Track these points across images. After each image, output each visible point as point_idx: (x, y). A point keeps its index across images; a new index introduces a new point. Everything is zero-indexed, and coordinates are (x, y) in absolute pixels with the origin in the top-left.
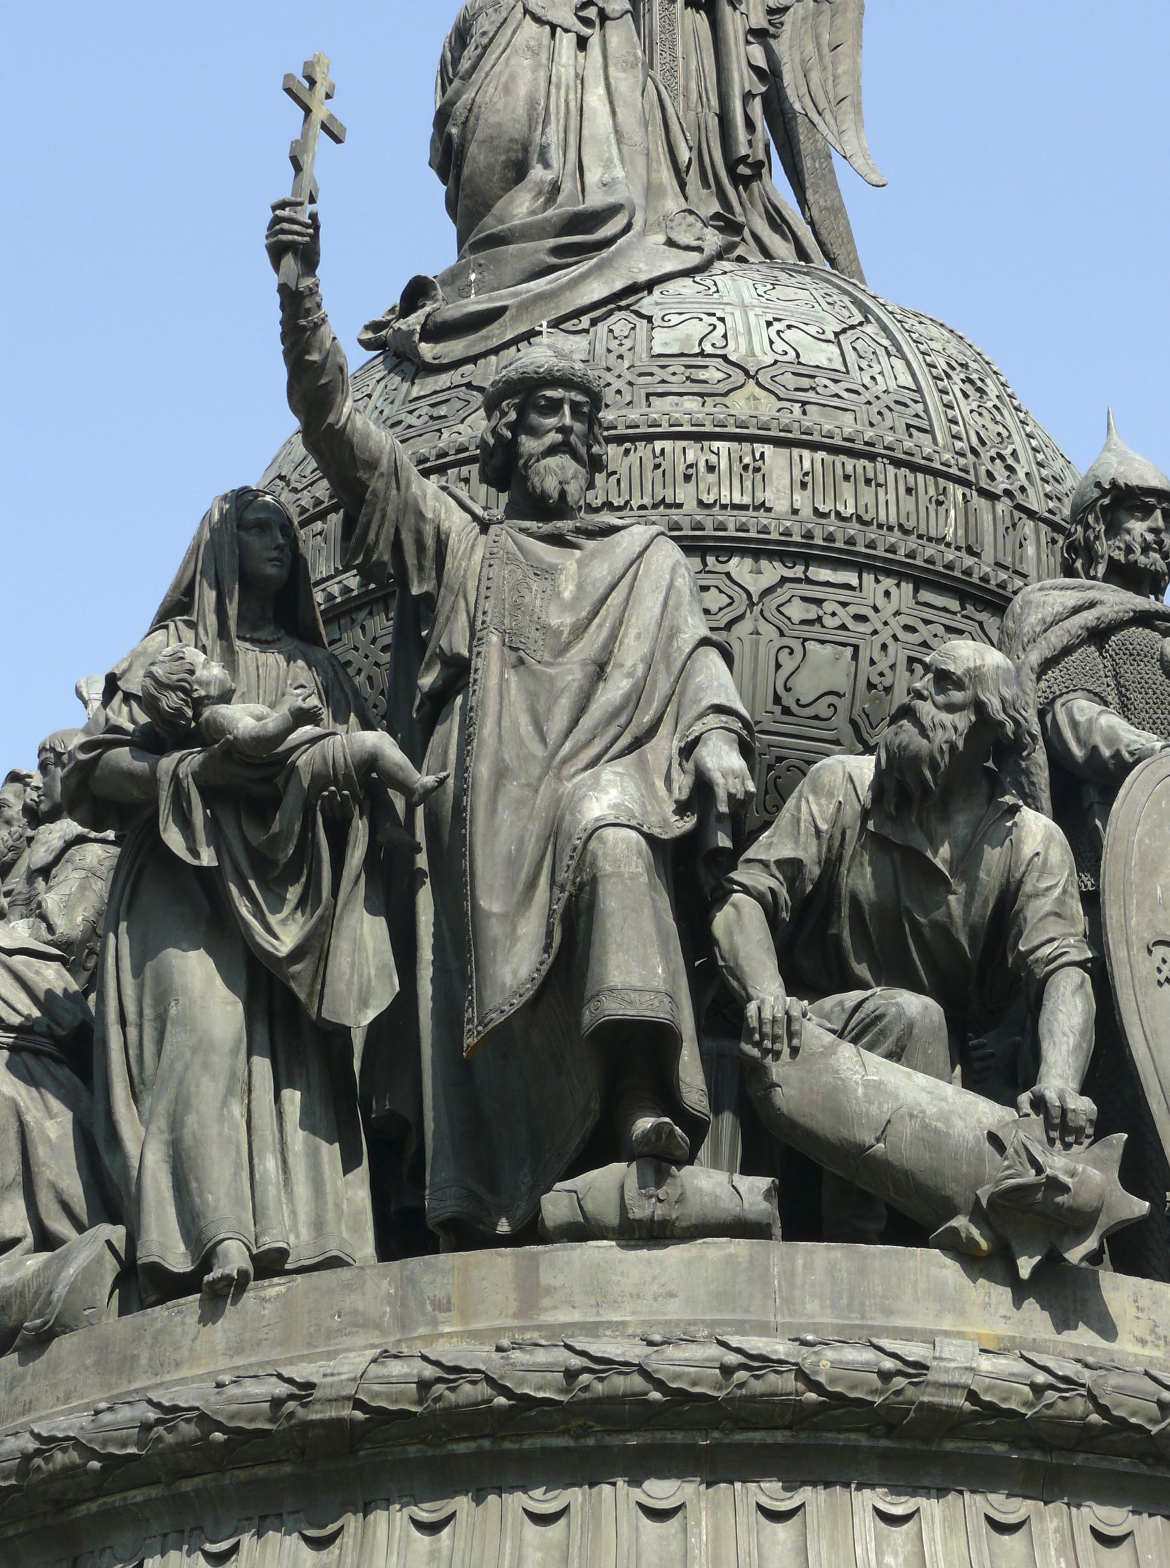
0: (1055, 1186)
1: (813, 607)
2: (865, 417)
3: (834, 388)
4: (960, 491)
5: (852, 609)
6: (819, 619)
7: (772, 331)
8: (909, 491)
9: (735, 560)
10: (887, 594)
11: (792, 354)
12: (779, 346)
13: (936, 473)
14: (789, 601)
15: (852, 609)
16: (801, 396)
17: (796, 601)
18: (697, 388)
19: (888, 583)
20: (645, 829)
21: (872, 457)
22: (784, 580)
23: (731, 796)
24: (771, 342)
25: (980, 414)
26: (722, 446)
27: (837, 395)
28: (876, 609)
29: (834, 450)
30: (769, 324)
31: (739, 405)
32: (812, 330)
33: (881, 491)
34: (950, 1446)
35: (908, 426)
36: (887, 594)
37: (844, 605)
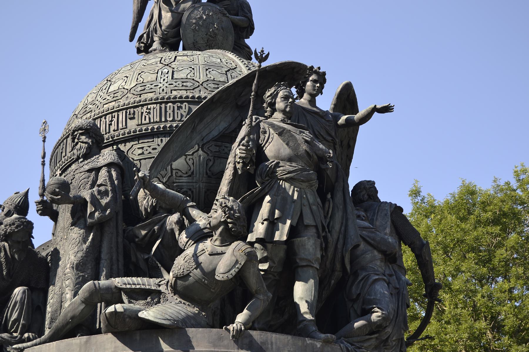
1: (141, 150)
5: (152, 147)
6: (143, 152)
7: (140, 75)
10: (162, 140)
12: (138, 81)
15: (152, 147)
16: (142, 92)
17: (137, 149)
18: (115, 99)
22: (133, 145)
24: (137, 79)
27: (151, 89)
28: (158, 145)
30: (139, 74)
35: (171, 90)
36: (162, 140)
37: (149, 147)
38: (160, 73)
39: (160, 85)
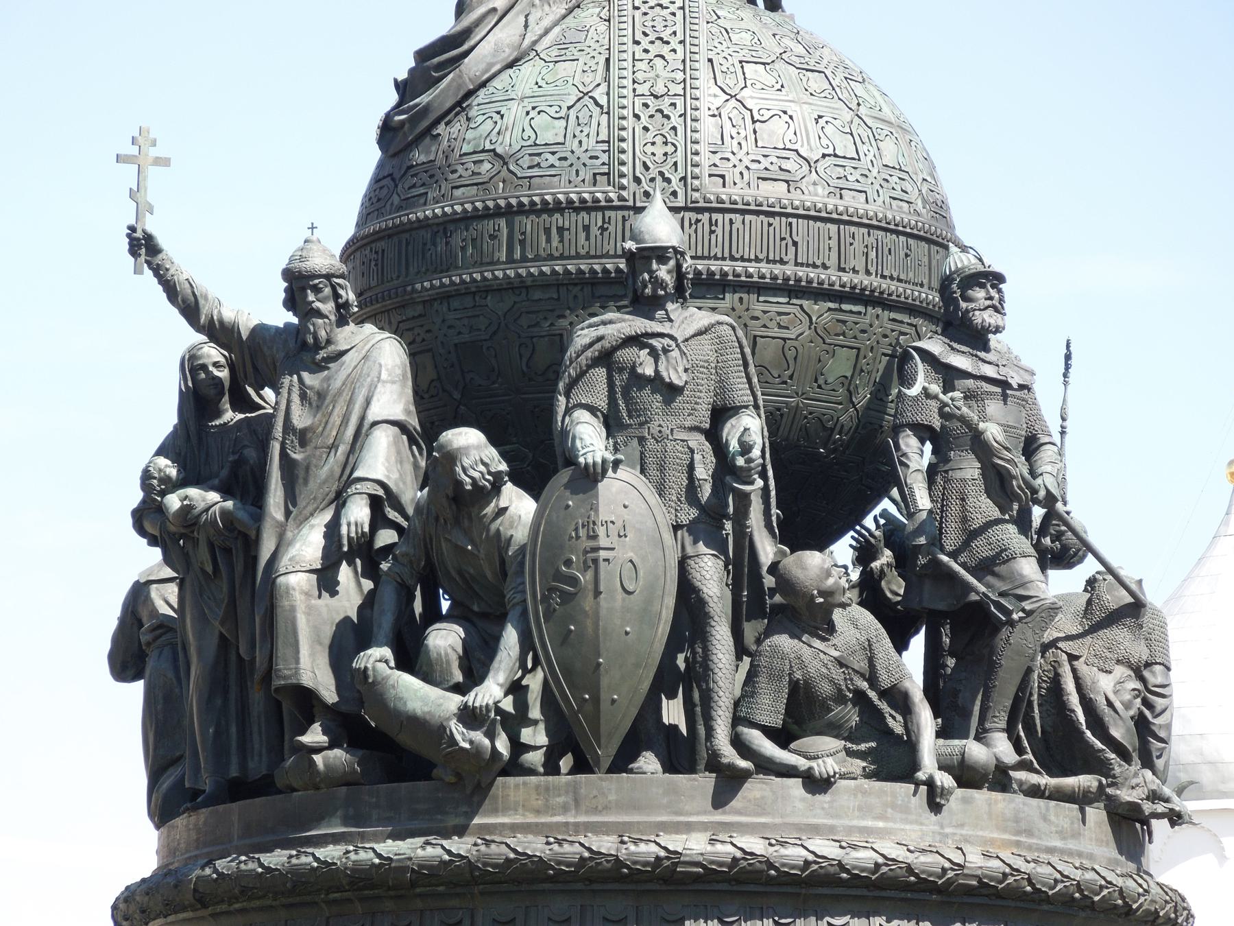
0: (463, 749)
2: (567, 178)
3: (552, 159)
4: (620, 214)
9: (489, 298)
10: (575, 297)
11: (533, 136)
13: (603, 209)
14: (519, 317)
19: (576, 290)
20: (309, 568)
23: (349, 538)
24: (524, 130)
25: (653, 144)
32: (552, 111)
33: (566, 233)
34: (418, 890)
39: (572, 159)
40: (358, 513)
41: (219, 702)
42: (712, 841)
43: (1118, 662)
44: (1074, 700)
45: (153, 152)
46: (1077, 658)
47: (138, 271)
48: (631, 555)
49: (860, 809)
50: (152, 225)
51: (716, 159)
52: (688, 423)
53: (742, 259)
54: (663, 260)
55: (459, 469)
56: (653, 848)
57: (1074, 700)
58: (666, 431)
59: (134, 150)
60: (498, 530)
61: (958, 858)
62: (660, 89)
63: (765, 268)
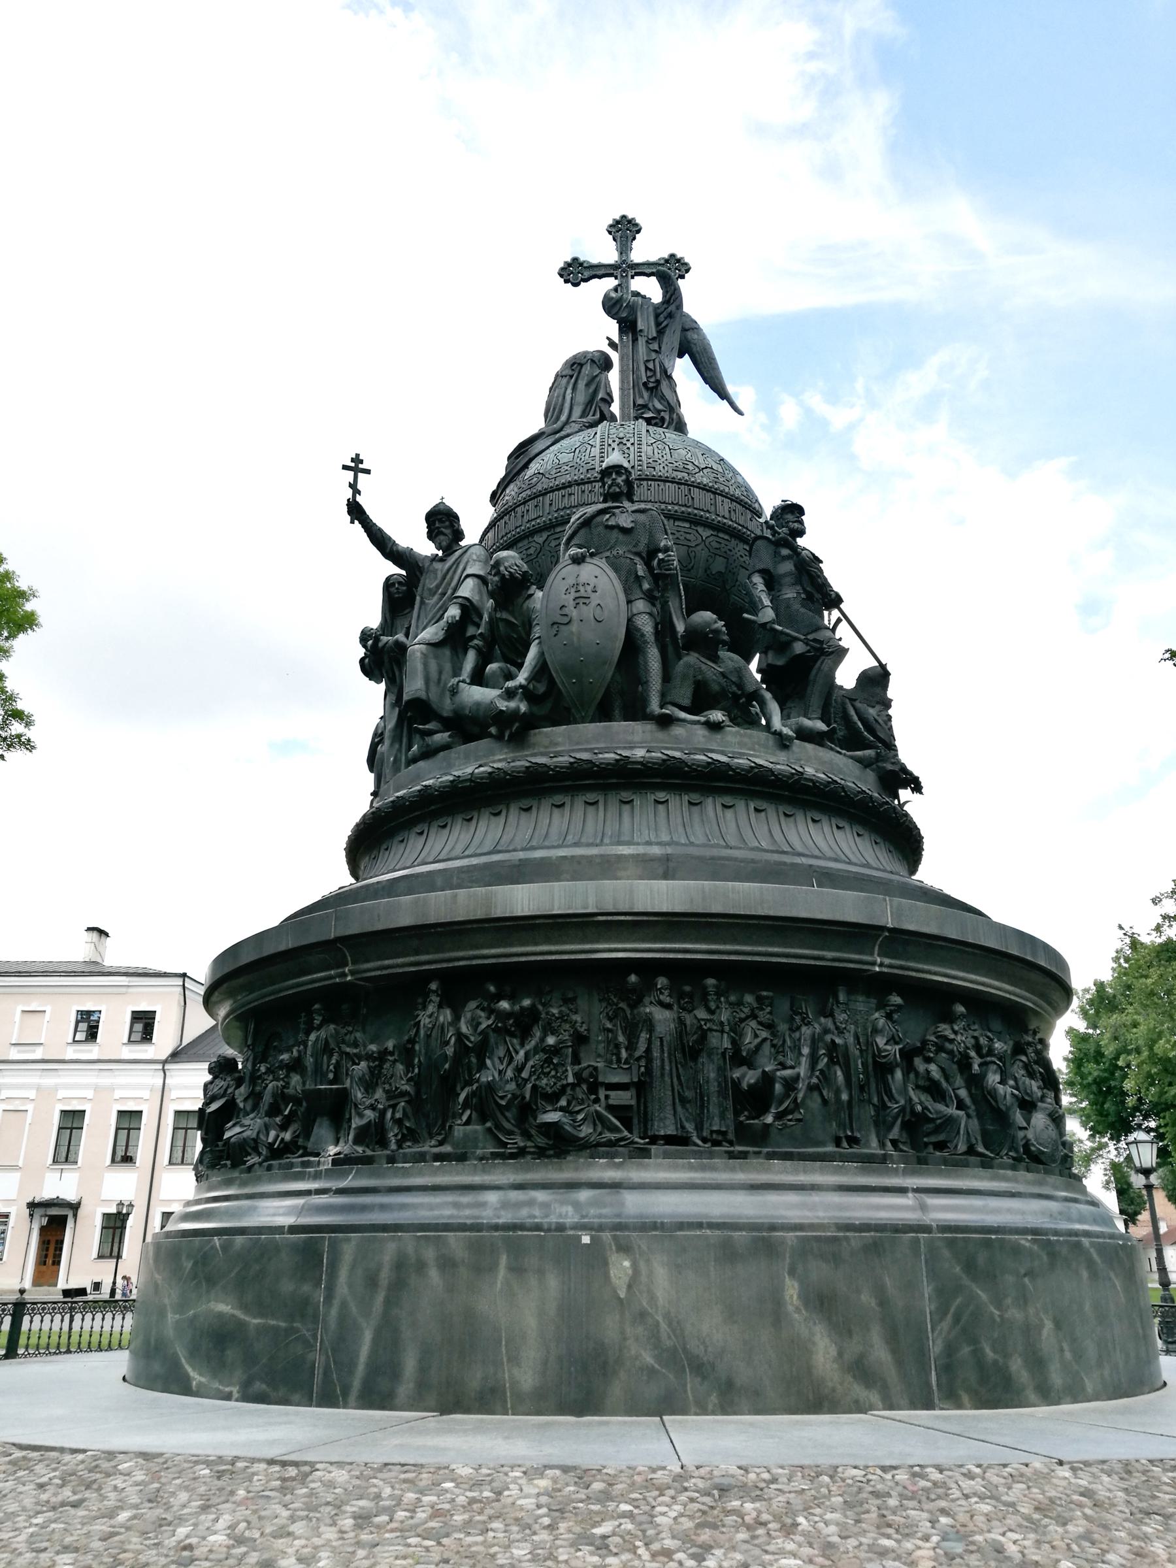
3: (566, 468)
8: (583, 492)
21: (570, 486)
26: (531, 504)
29: (558, 489)
31: (539, 487)
38: (577, 450)
40: (454, 612)
41: (397, 746)
42: (648, 751)
43: (878, 703)
44: (855, 718)
45: (361, 466)
46: (855, 700)
47: (352, 522)
48: (598, 602)
49: (739, 743)
50: (358, 499)
51: (650, 461)
52: (634, 550)
53: (664, 503)
54: (619, 474)
55: (502, 568)
56: (612, 755)
57: (855, 718)
58: (620, 552)
59: (353, 465)
60: (528, 607)
61: (800, 770)
62: (621, 435)
63: (676, 508)
